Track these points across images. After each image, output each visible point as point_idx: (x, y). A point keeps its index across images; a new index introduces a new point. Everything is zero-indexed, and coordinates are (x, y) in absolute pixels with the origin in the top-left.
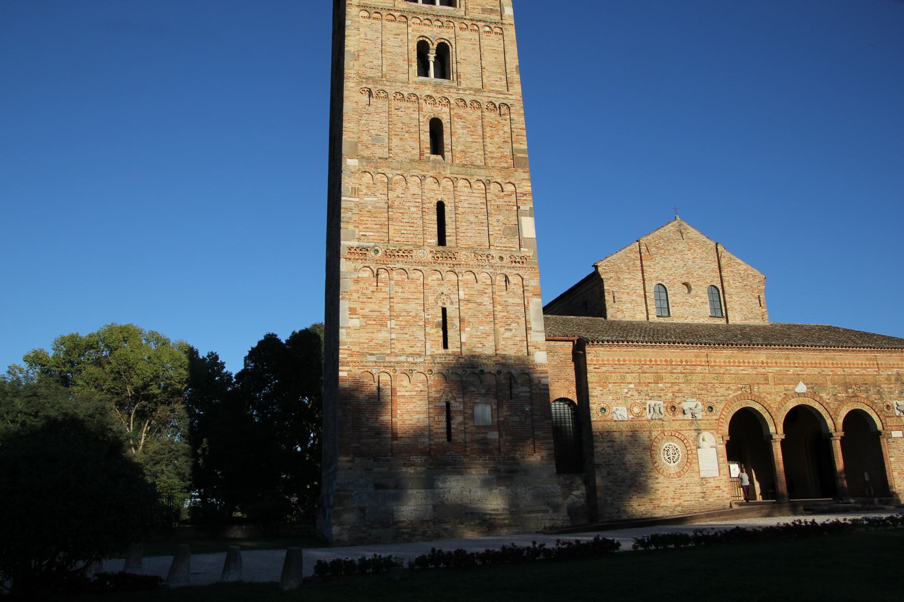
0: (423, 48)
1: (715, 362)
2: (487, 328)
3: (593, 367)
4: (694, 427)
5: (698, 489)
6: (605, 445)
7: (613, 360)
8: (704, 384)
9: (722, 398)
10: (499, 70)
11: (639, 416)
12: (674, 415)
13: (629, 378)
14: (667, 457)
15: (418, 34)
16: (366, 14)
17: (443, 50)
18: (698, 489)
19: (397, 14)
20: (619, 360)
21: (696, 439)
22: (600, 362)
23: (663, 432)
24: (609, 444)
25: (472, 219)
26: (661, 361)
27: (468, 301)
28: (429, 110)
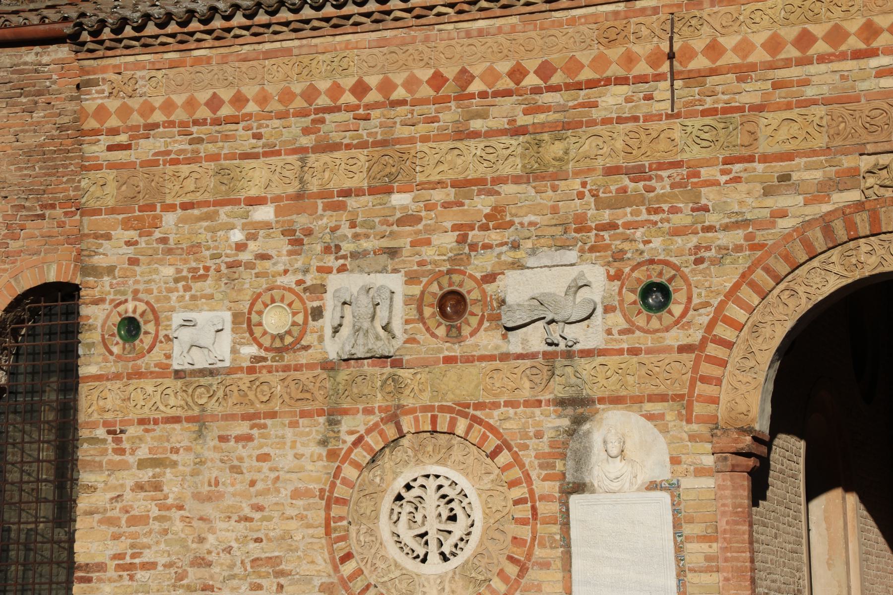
1: (714, 49)
3: (105, 140)
4: (557, 390)
6: (129, 478)
7: (191, 104)
8: (638, 173)
9: (737, 236)
11: (283, 346)
12: (454, 334)
13: (257, 177)
14: (408, 537)
20: (214, 103)
21: (571, 444)
22: (136, 119)
23: (393, 417)
24: (146, 475)
26: (411, 83)
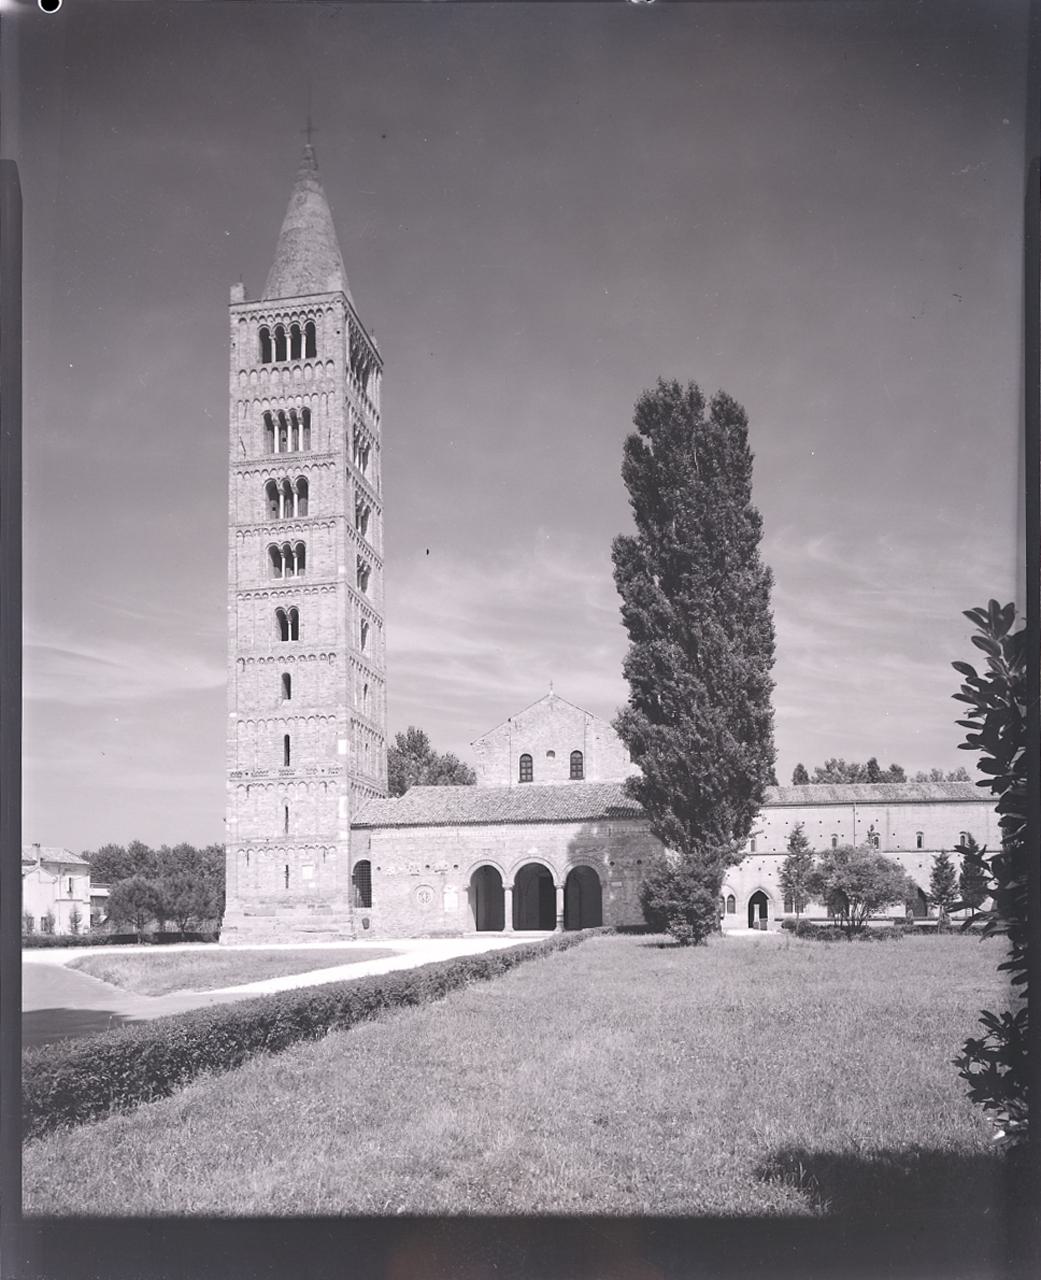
0: (280, 614)
2: (312, 818)
5: (441, 920)
10: (331, 625)
15: (276, 607)
16: (240, 597)
17: (295, 613)
18: (441, 920)
19: (261, 593)
25: (306, 745)
27: (302, 801)
28: (284, 668)
